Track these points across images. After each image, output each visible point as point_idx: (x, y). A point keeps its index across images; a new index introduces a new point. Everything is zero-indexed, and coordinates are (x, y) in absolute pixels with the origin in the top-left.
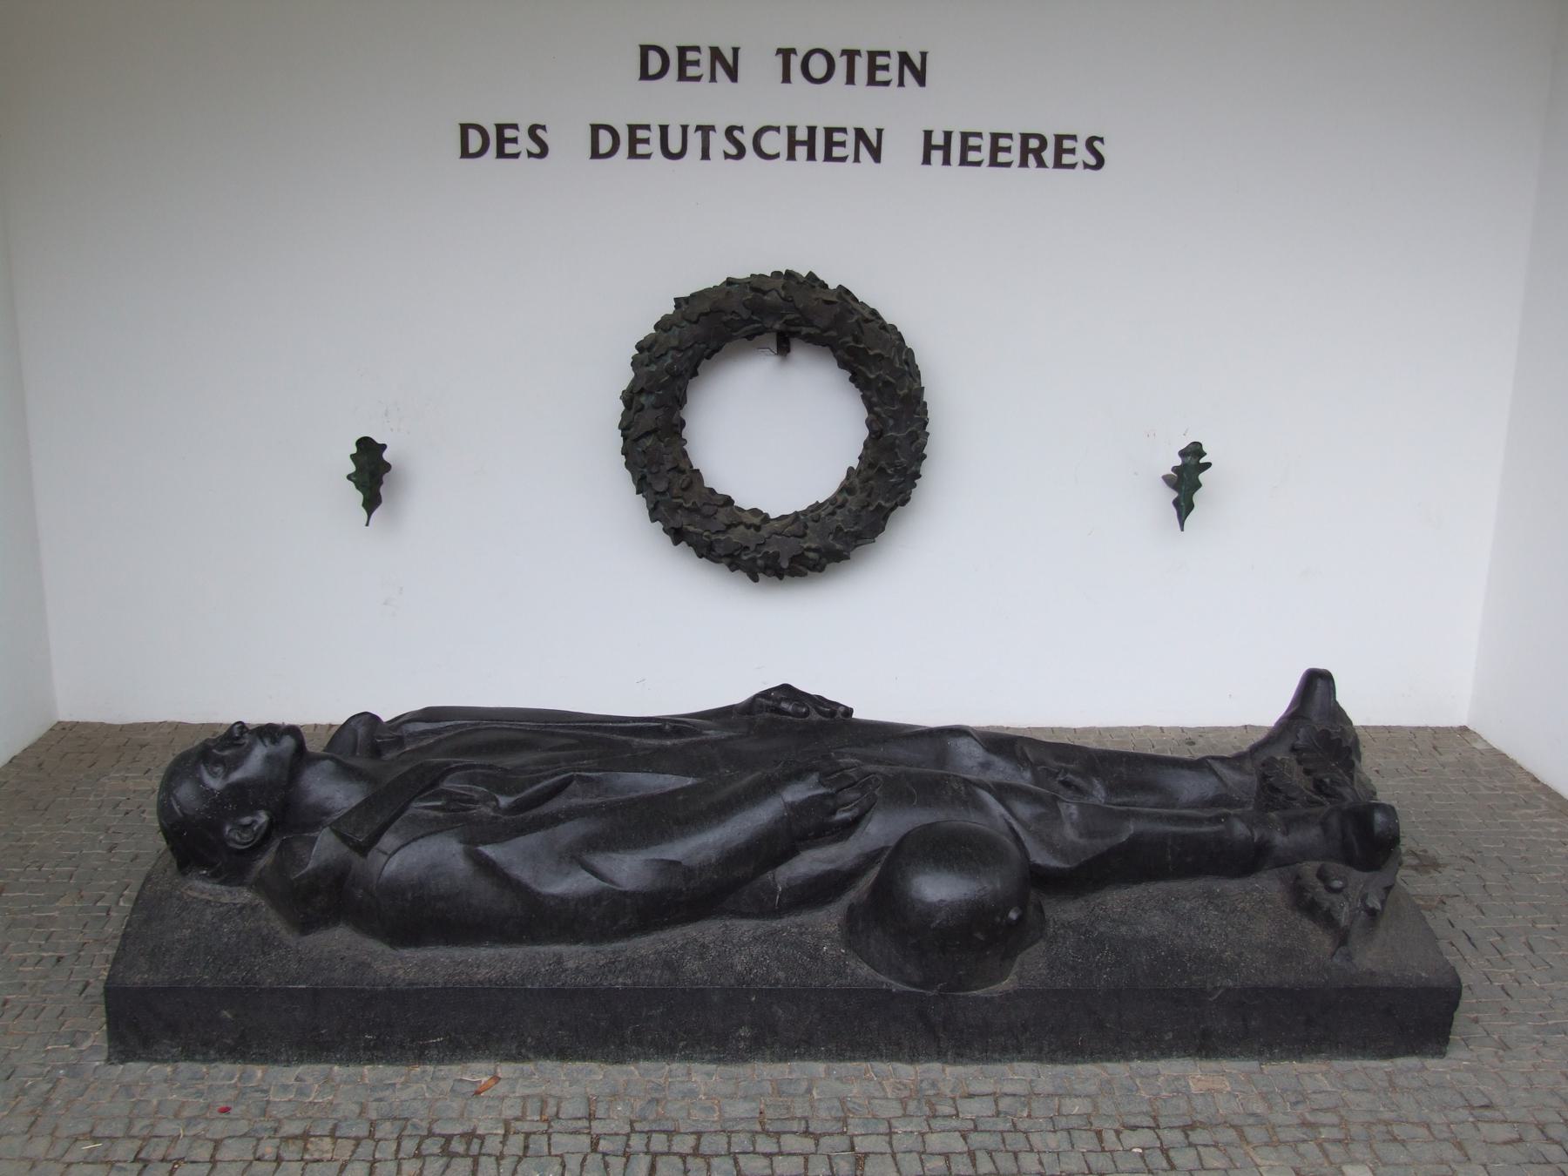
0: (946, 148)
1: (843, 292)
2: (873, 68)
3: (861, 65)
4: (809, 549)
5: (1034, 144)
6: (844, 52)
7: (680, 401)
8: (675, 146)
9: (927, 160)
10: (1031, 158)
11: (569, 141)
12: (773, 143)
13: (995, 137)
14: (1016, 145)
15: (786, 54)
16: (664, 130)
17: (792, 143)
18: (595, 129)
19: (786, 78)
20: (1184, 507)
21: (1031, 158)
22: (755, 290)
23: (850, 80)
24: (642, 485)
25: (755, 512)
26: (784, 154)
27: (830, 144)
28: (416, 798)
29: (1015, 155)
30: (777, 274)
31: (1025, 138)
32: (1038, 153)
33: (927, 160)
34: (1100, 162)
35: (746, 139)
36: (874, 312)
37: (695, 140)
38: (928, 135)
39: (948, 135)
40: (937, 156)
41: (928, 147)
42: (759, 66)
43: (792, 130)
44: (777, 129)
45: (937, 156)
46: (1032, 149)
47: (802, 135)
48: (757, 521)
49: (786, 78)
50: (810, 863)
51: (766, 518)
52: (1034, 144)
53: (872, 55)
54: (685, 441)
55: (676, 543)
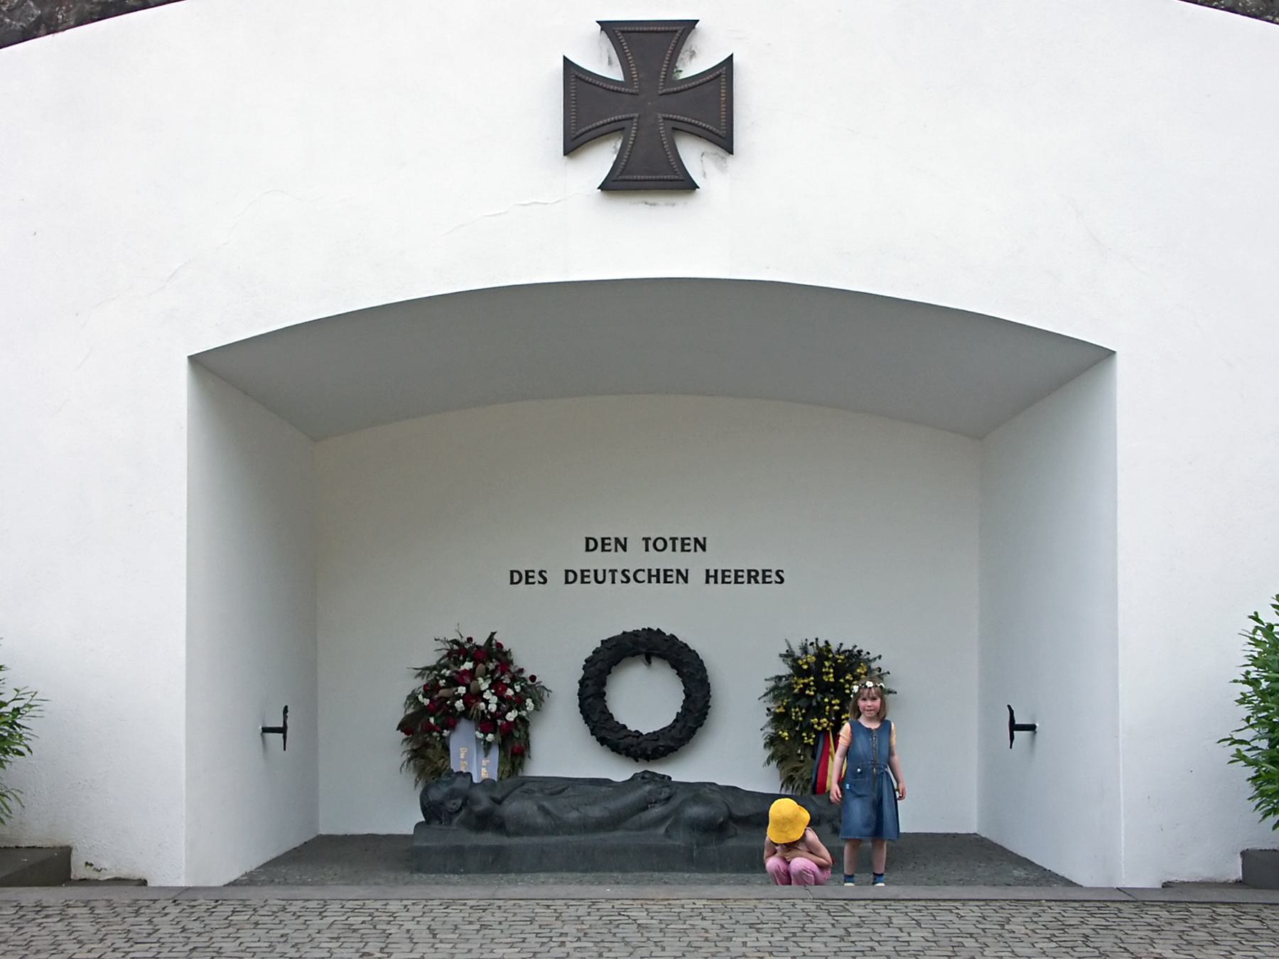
0: (715, 577)
1: (673, 636)
2: (683, 544)
3: (678, 543)
4: (660, 746)
5: (753, 574)
6: (671, 539)
7: (604, 684)
8: (600, 579)
9: (707, 582)
10: (752, 580)
11: (556, 577)
12: (642, 576)
13: (736, 571)
14: (745, 574)
15: (647, 540)
16: (596, 571)
17: (650, 576)
18: (567, 572)
19: (647, 550)
21: (752, 580)
22: (636, 635)
23: (674, 550)
24: (587, 719)
25: (637, 731)
26: (647, 581)
27: (666, 576)
28: (517, 792)
30: (644, 629)
31: (749, 571)
33: (707, 582)
34: (782, 580)
35: (631, 575)
36: (686, 645)
37: (609, 575)
38: (708, 571)
39: (716, 571)
40: (712, 580)
41: (708, 576)
42: (635, 545)
44: (644, 571)
45: (712, 580)
46: (752, 576)
48: (637, 735)
49: (647, 550)
51: (641, 734)
52: (753, 574)
53: (683, 539)
54: (605, 701)
55: (602, 745)
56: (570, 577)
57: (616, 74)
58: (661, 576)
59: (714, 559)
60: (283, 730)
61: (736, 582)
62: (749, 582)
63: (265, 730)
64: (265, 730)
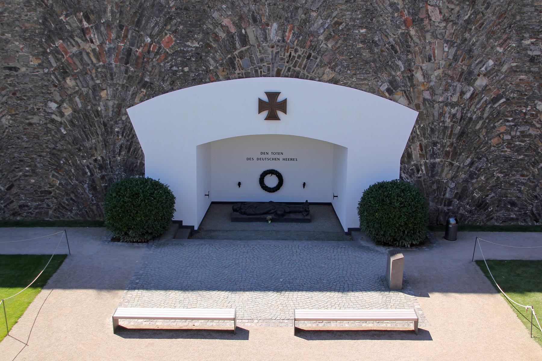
11: (255, 159)
20: (304, 187)
42: (270, 153)
46: (291, 159)
50: (273, 211)
56: (258, 159)
58: (275, 159)
59: (284, 156)
60: (208, 195)
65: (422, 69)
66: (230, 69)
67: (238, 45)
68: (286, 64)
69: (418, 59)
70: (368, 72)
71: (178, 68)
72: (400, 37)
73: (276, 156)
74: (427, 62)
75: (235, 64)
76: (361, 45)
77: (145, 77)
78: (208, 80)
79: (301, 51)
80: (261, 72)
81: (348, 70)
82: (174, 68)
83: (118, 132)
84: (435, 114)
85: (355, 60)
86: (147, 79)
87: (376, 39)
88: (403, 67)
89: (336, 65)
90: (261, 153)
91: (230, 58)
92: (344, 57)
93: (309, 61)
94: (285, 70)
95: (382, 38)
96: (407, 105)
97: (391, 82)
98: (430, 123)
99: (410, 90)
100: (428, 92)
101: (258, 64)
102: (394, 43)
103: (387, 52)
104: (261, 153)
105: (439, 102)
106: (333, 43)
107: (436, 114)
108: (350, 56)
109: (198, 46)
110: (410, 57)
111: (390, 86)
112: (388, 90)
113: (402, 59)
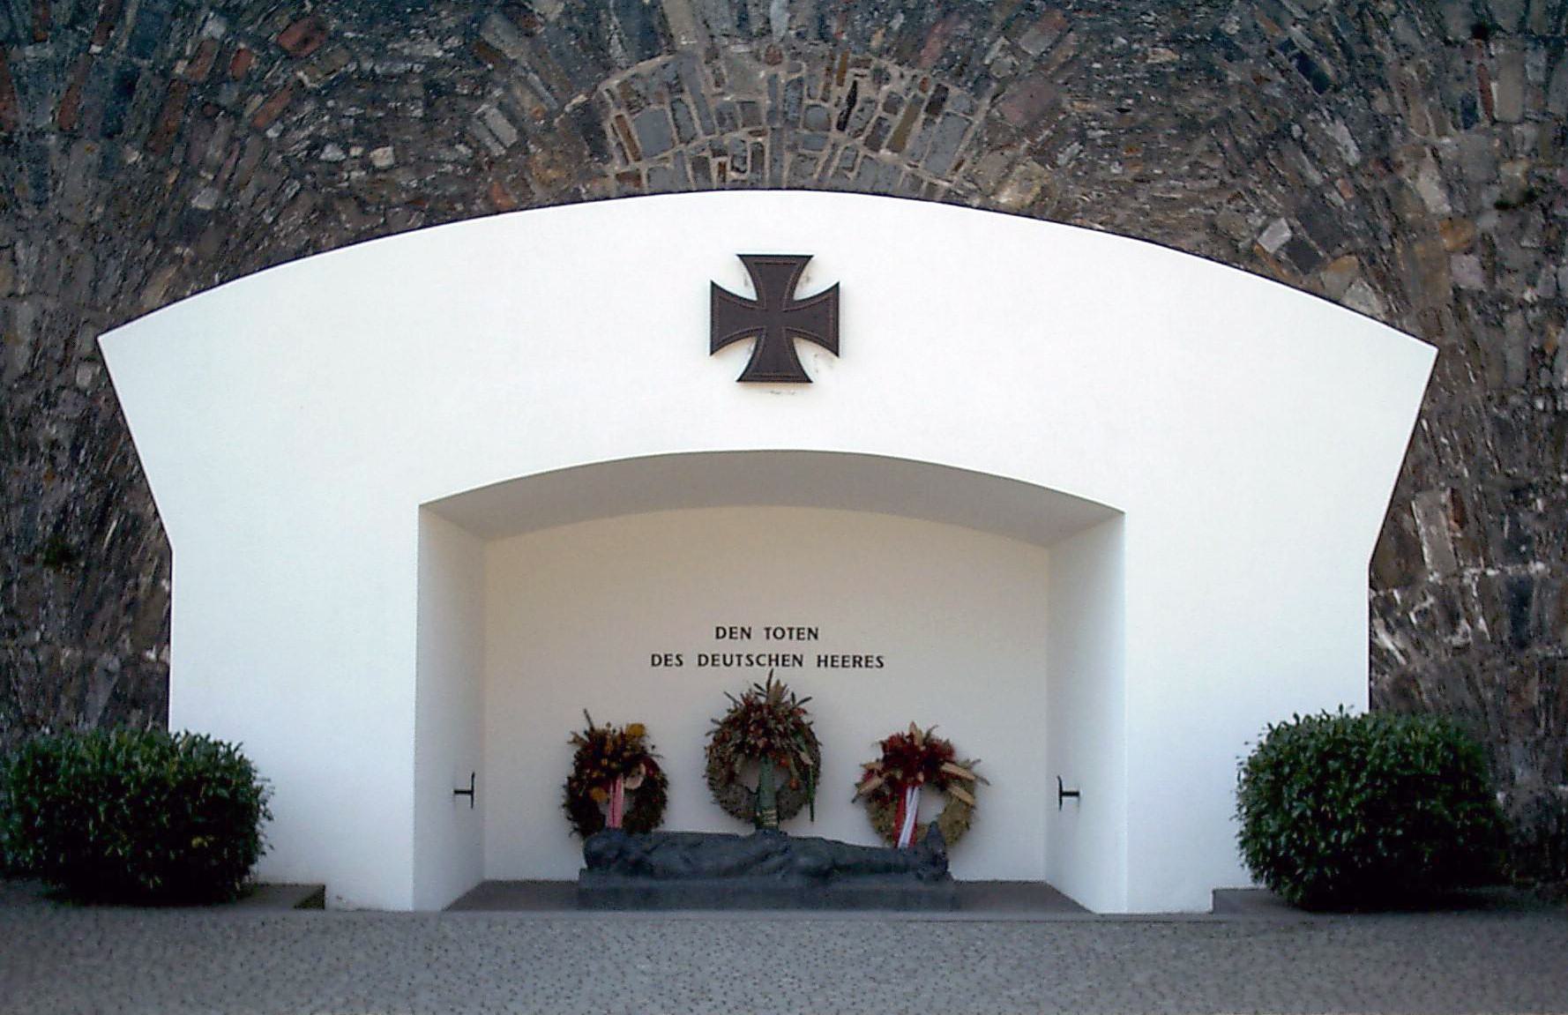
3: (795, 633)
8: (728, 661)
9: (819, 665)
11: (690, 660)
12: (763, 660)
13: (844, 657)
15: (768, 629)
16: (724, 656)
17: (770, 660)
18: (700, 656)
19: (768, 637)
23: (791, 637)
29: (851, 663)
31: (854, 657)
32: (859, 663)
33: (819, 665)
35: (754, 659)
37: (735, 659)
38: (819, 657)
40: (822, 664)
41: (819, 661)
43: (770, 656)
45: (822, 664)
46: (857, 661)
47: (774, 657)
49: (768, 637)
52: (858, 659)
53: (799, 629)
56: (702, 660)
57: (749, 293)
61: (843, 666)
62: (854, 666)
63: (457, 792)
64: (457, 792)
65: (1439, 162)
66: (580, 156)
67: (616, 50)
68: (834, 134)
69: (1421, 115)
70: (1202, 172)
71: (346, 151)
72: (1336, 24)
73: (788, 647)
74: (1456, 127)
75: (603, 133)
76: (1164, 55)
77: (194, 192)
78: (479, 204)
79: (902, 76)
80: (722, 166)
81: (1111, 161)
82: (331, 153)
83: (54, 444)
84: (1510, 356)
85: (1144, 116)
86: (203, 201)
87: (1232, 28)
88: (1353, 148)
89: (1061, 138)
90: (720, 633)
91: (585, 107)
92: (1092, 107)
93: (939, 120)
94: (829, 161)
95: (1256, 26)
96: (1383, 317)
97: (1305, 217)
98: (1490, 399)
99: (1393, 251)
100: (1473, 260)
101: (707, 134)
102: (1309, 44)
103: (1280, 85)
104: (720, 633)
105: (1522, 305)
106: (1043, 45)
107: (1517, 361)
108: (1121, 98)
109: (439, 54)
110: (1381, 105)
111: (1303, 233)
112: (1294, 248)
113: (1351, 115)
